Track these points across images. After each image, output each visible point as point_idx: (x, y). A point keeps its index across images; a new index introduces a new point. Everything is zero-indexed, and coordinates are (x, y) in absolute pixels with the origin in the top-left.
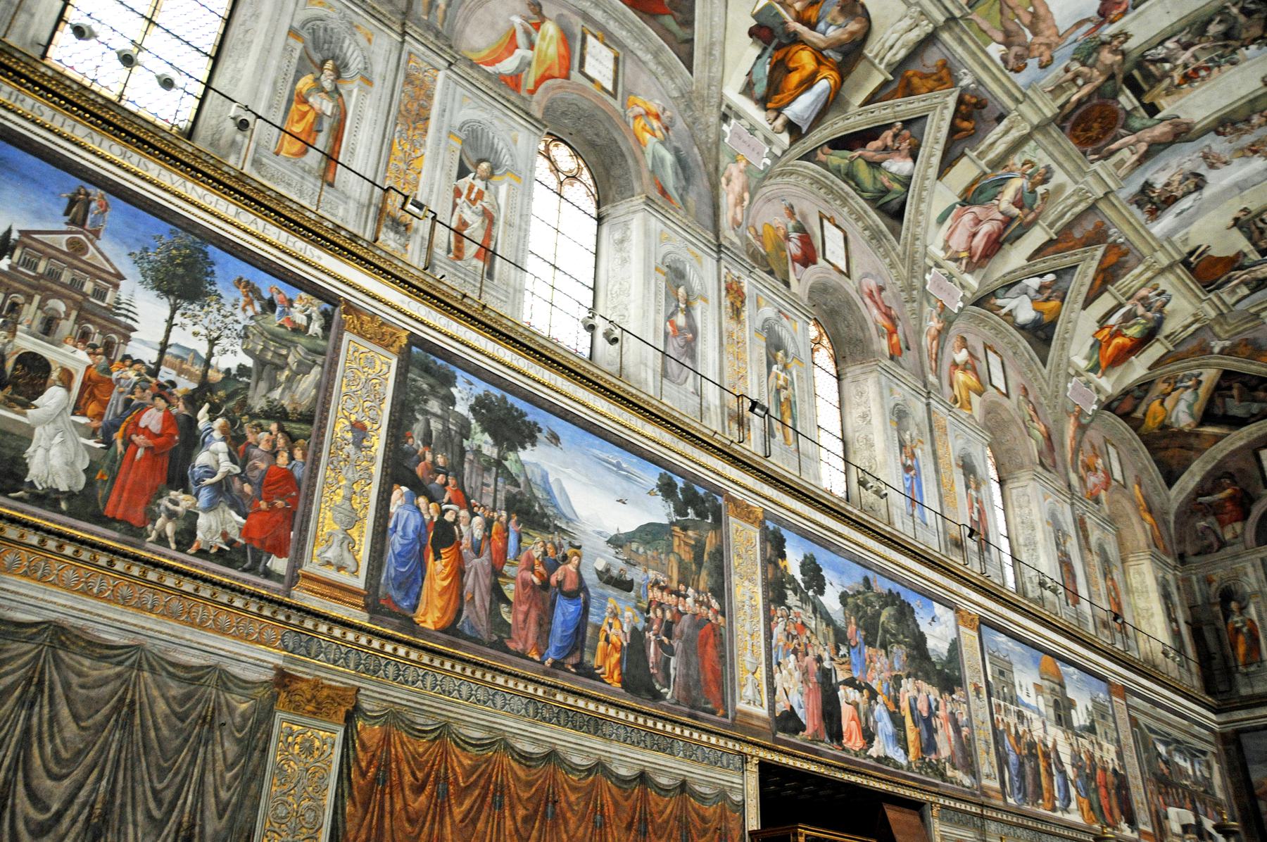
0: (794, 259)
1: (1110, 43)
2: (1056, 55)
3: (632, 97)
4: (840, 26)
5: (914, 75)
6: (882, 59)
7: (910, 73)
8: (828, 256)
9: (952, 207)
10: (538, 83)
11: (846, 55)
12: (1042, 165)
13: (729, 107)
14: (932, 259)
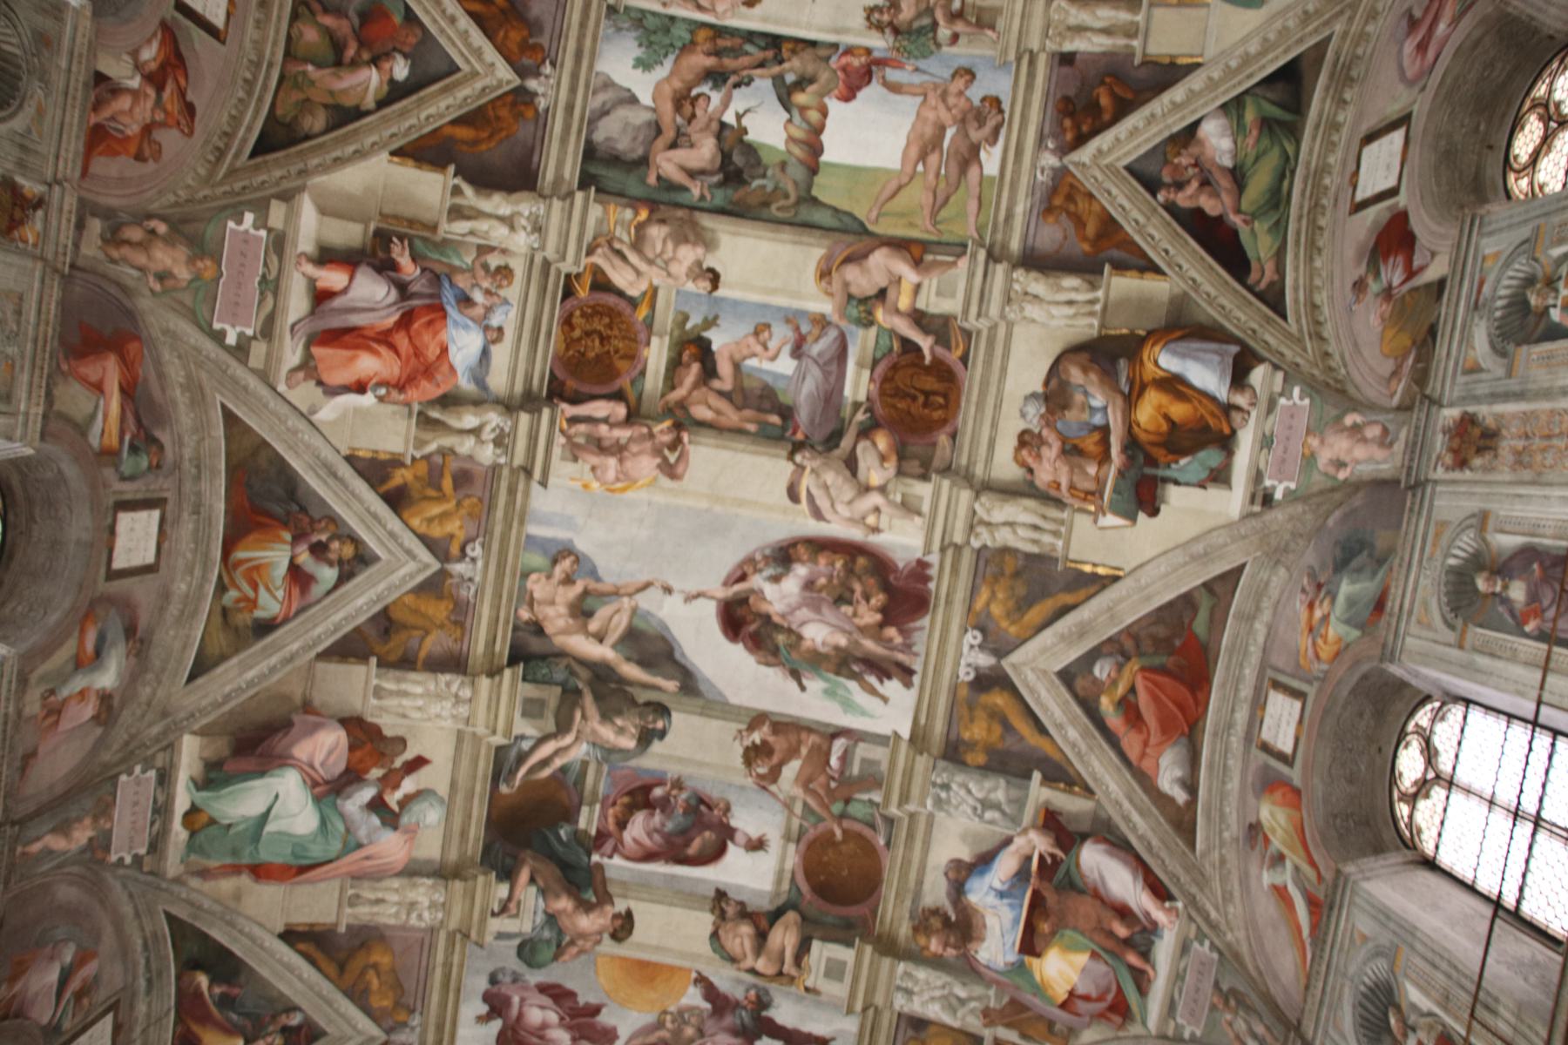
0: (1411, 273)
1: (890, 24)
2: (947, 74)
3: (1302, 661)
4: (1086, 393)
5: (1085, 239)
6: (1092, 302)
7: (1086, 247)
8: (1391, 182)
10: (1313, 864)
11: (1113, 360)
13: (1252, 501)
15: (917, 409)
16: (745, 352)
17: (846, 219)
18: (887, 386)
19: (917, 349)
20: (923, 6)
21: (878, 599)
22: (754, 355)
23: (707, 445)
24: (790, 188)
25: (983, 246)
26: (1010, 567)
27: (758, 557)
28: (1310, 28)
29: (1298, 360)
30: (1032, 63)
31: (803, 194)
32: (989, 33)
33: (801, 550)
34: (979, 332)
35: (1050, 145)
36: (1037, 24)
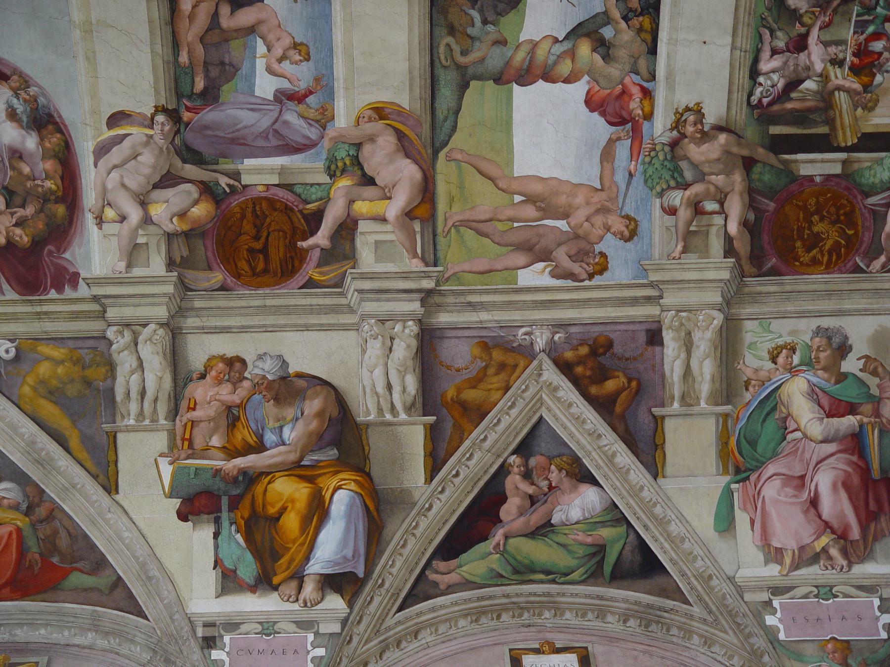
1: (683, 136)
2: (629, 209)
5: (459, 390)
6: (393, 408)
7: (451, 393)
9: (728, 493)
11: (336, 443)
12: (807, 338)
13: (206, 625)
14: (760, 589)
15: (245, 241)
16: (271, 37)
18: (264, 204)
19: (313, 232)
20: (706, 170)
21: (22, 237)
22: (269, 50)
23: (148, 9)
24: (475, 55)
25: (438, 284)
26: (97, 373)
27: (33, 90)
28: (695, 583)
29: (355, 640)
30: (649, 299)
31: (470, 71)
32: (680, 248)
33: (56, 139)
34: (343, 295)
35: (556, 337)
36: (692, 297)
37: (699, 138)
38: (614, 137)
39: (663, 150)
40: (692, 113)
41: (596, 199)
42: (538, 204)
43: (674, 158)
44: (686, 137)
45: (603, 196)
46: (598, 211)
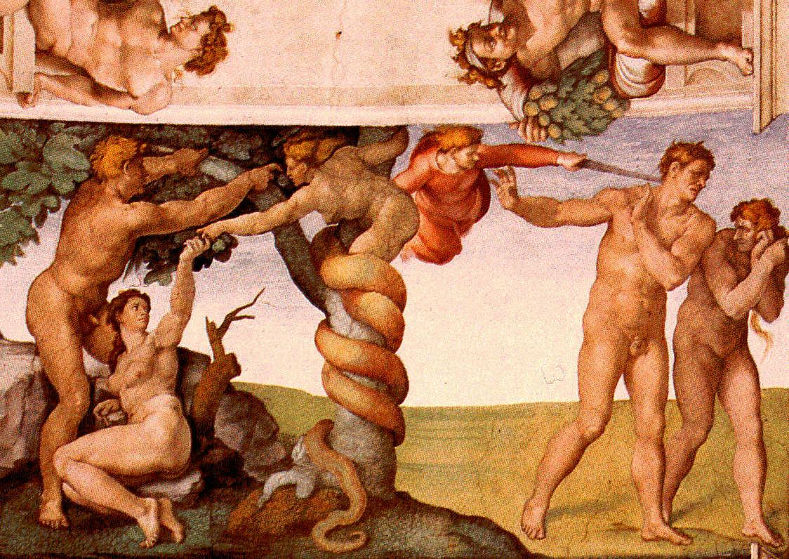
1: (512, 62)
2: (649, 163)
17: (476, 534)
20: (578, 11)
37: (517, 31)
38: (510, 201)
39: (537, 101)
40: (468, 48)
41: (629, 236)
42: (633, 350)
43: (555, 78)
44: (514, 56)
45: (621, 217)
46: (652, 228)
